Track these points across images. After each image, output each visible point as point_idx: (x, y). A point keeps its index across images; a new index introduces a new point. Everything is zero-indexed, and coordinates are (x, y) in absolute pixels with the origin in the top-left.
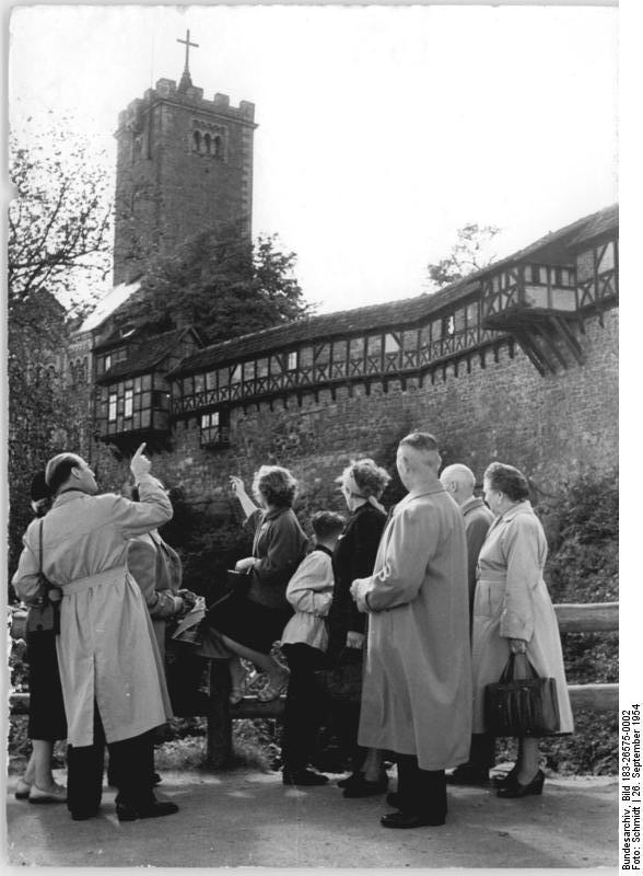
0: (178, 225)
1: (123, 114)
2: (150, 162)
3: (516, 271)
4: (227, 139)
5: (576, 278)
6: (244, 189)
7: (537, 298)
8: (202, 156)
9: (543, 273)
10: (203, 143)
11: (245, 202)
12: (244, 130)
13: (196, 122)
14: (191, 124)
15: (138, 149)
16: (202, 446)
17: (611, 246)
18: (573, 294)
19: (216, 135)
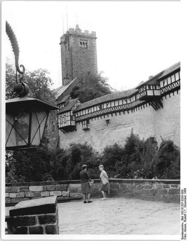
0: (78, 68)
1: (61, 38)
2: (69, 51)
3: (145, 87)
4: (89, 43)
5: (160, 87)
6: (94, 56)
7: (150, 93)
8: (82, 48)
9: (151, 87)
10: (83, 44)
11: (95, 59)
12: (93, 40)
13: (80, 39)
14: (79, 39)
15: (66, 47)
16: (83, 129)
17: (166, 79)
18: (159, 91)
19: (86, 42)
